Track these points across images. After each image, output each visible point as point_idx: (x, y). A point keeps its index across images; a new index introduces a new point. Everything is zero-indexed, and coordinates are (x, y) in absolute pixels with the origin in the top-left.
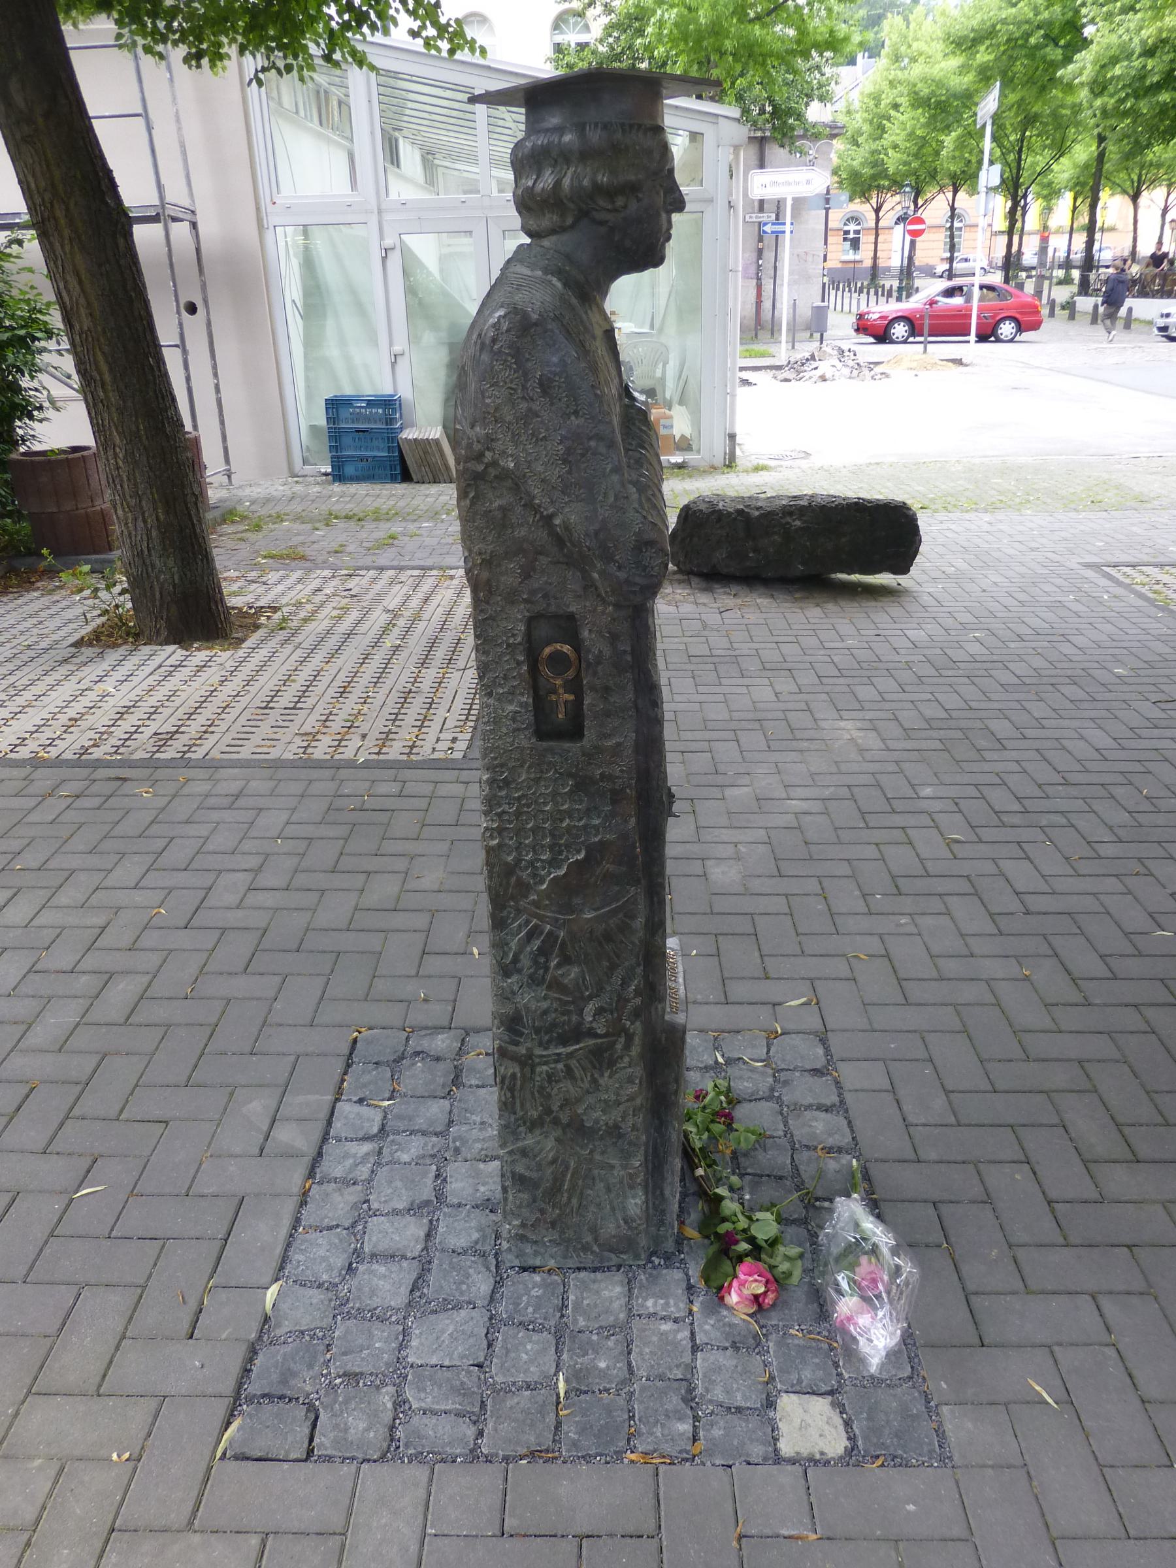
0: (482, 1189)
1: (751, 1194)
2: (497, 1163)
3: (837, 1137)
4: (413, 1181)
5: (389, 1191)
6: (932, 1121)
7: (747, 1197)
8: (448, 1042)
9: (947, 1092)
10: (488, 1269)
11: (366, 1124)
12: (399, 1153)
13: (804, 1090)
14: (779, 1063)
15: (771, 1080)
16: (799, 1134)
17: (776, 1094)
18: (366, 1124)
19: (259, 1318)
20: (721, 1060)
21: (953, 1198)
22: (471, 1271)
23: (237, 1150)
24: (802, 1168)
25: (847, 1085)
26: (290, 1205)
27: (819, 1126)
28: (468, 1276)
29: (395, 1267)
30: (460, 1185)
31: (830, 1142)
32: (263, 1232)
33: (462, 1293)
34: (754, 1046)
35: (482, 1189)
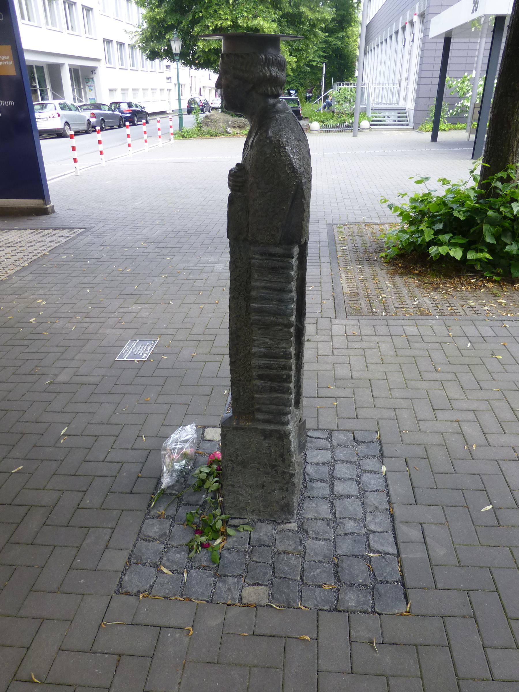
0: (314, 505)
1: (202, 497)
2: (309, 516)
3: (151, 523)
4: (345, 509)
5: (354, 506)
6: (101, 530)
7: (204, 496)
8: (347, 598)
9: (79, 548)
10: (308, 474)
11: (376, 539)
12: (356, 525)
13: (150, 550)
14: (154, 571)
15: (165, 559)
16: (167, 524)
17: (165, 550)
18: (376, 539)
19: (384, 463)
20: (185, 575)
21: (122, 494)
22: (314, 474)
23: (433, 527)
24: (175, 509)
25: (126, 554)
26: (394, 499)
27: (154, 528)
28: (315, 472)
29: (343, 476)
30: (324, 509)
31: (155, 521)
32: (400, 490)
33: (316, 467)
34: (162, 584)
35: (314, 505)
